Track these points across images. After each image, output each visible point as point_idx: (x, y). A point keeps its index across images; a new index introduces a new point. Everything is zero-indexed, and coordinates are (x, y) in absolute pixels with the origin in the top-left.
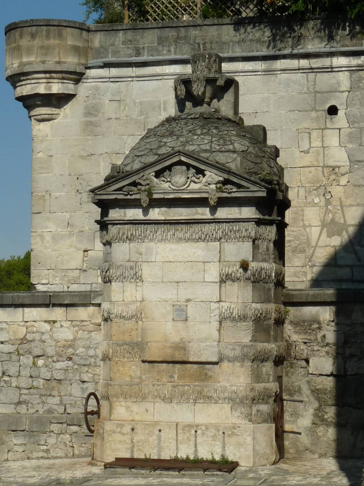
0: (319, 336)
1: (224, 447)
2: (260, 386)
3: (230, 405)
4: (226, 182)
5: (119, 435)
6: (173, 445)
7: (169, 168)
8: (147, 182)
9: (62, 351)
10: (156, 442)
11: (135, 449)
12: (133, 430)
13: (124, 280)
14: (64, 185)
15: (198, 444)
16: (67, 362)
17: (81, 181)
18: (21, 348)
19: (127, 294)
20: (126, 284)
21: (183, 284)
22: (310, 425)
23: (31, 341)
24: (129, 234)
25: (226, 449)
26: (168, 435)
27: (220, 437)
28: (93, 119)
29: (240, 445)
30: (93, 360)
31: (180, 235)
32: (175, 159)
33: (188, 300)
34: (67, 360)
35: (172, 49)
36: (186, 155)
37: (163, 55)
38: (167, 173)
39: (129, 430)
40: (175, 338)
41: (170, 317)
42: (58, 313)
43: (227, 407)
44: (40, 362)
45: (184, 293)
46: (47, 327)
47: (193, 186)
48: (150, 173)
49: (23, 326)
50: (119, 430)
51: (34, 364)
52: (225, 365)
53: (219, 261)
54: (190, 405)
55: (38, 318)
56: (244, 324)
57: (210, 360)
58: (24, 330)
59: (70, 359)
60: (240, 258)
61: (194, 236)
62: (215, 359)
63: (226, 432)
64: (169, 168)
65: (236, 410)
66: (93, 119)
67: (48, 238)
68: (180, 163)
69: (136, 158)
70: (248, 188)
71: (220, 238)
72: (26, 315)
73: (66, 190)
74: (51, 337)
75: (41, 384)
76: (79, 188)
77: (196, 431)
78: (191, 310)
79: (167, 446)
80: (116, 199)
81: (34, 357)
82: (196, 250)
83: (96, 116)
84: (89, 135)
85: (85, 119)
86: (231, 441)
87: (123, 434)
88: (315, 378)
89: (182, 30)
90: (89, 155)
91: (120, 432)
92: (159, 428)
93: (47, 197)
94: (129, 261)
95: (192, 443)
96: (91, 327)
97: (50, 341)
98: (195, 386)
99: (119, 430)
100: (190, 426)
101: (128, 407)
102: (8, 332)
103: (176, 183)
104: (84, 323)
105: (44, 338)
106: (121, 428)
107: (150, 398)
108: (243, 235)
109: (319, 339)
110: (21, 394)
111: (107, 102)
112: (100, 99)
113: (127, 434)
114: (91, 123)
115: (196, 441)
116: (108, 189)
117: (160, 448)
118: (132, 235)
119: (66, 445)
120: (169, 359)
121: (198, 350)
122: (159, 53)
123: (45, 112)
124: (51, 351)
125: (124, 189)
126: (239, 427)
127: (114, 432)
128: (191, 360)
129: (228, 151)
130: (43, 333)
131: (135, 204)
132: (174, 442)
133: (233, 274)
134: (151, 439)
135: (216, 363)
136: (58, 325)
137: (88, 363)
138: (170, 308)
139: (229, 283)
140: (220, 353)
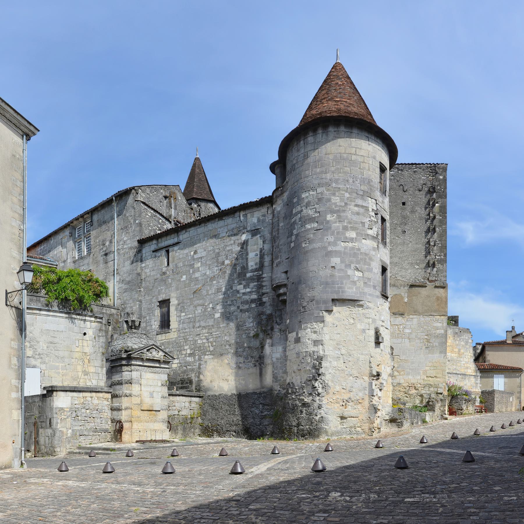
30: (104, 410)
42: (94, 394)
44: (88, 411)
46: (90, 399)
59: (97, 410)
124: (91, 408)
136: (93, 398)
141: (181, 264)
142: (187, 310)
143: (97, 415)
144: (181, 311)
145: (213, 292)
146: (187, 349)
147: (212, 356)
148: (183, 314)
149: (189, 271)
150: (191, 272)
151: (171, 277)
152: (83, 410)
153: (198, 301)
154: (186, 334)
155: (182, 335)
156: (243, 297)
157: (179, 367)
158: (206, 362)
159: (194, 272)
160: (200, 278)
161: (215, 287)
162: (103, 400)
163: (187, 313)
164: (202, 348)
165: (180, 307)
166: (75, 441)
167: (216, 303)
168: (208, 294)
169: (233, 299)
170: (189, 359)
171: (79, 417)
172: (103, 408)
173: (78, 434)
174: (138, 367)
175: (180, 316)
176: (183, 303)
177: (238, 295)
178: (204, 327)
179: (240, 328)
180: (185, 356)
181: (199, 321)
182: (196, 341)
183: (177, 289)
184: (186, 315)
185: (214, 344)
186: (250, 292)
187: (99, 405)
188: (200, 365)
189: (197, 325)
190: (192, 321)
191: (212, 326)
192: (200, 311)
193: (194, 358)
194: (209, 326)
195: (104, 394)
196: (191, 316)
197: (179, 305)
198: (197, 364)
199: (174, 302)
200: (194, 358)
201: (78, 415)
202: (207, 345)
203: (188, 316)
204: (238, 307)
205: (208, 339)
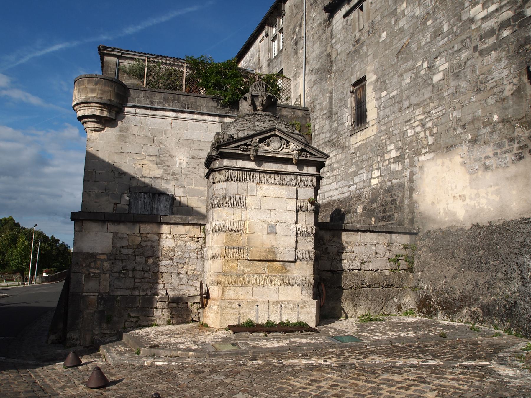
3: (300, 288)
4: (303, 150)
7: (269, 137)
9: (166, 254)
10: (255, 313)
11: (241, 319)
12: (240, 305)
15: (282, 314)
16: (169, 261)
18: (137, 251)
19: (236, 215)
20: (235, 209)
25: (300, 316)
28: (124, 134)
31: (271, 180)
32: (272, 133)
33: (277, 221)
34: (169, 259)
35: (171, 104)
36: (280, 130)
37: (166, 106)
39: (237, 306)
41: (266, 232)
43: (298, 289)
45: (274, 218)
47: (285, 151)
48: (257, 139)
49: (139, 236)
50: (230, 306)
51: (146, 261)
54: (275, 288)
55: (150, 231)
56: (309, 238)
57: (290, 260)
58: (140, 239)
59: (172, 259)
60: (307, 198)
64: (269, 137)
65: (304, 292)
66: (124, 134)
67: (93, 195)
68: (275, 135)
69: (238, 131)
72: (142, 229)
75: (150, 275)
78: (280, 229)
79: (263, 316)
81: (146, 258)
82: (282, 191)
83: (126, 132)
84: (121, 142)
85: (120, 133)
87: (233, 309)
89: (177, 95)
90: (120, 153)
91: (231, 308)
94: (237, 194)
96: (187, 239)
99: (230, 306)
100: (278, 302)
101: (235, 291)
102: (128, 240)
103: (275, 147)
104: (182, 236)
106: (232, 305)
109: (324, 250)
110: (135, 282)
111: (133, 126)
114: (123, 136)
115: (281, 311)
116: (230, 146)
117: (258, 318)
118: (240, 178)
121: (283, 253)
122: (163, 105)
123: (97, 126)
126: (308, 302)
127: (227, 307)
128: (278, 259)
130: (153, 242)
131: (247, 158)
137: (184, 262)
138: (265, 226)
141: (379, 18)
142: (389, 86)
144: (381, 90)
145: (429, 40)
146: (391, 151)
147: (431, 155)
148: (384, 93)
149: (390, 22)
150: (393, 23)
151: (367, 42)
153: (405, 64)
154: (389, 124)
155: (383, 128)
156: (483, 25)
157: (380, 183)
158: (422, 167)
159: (396, 22)
160: (406, 27)
161: (431, 30)
163: (390, 90)
164: (414, 144)
165: (379, 83)
167: (434, 56)
168: (420, 48)
169: (464, 37)
170: (395, 167)
175: (380, 98)
176: (383, 75)
177: (473, 27)
178: (417, 105)
179: (482, 87)
180: (390, 163)
181: (408, 97)
182: (405, 132)
183: (375, 57)
184: (387, 94)
185: (435, 130)
186: (497, 10)
188: (412, 174)
189: (406, 104)
190: (398, 101)
191: (430, 98)
192: (408, 80)
193: (403, 163)
194: (425, 100)
196: (395, 93)
197: (377, 80)
198: (408, 174)
199: (371, 78)
200: (403, 163)
202: (422, 135)
203: (392, 95)
204: (475, 48)
205: (423, 125)
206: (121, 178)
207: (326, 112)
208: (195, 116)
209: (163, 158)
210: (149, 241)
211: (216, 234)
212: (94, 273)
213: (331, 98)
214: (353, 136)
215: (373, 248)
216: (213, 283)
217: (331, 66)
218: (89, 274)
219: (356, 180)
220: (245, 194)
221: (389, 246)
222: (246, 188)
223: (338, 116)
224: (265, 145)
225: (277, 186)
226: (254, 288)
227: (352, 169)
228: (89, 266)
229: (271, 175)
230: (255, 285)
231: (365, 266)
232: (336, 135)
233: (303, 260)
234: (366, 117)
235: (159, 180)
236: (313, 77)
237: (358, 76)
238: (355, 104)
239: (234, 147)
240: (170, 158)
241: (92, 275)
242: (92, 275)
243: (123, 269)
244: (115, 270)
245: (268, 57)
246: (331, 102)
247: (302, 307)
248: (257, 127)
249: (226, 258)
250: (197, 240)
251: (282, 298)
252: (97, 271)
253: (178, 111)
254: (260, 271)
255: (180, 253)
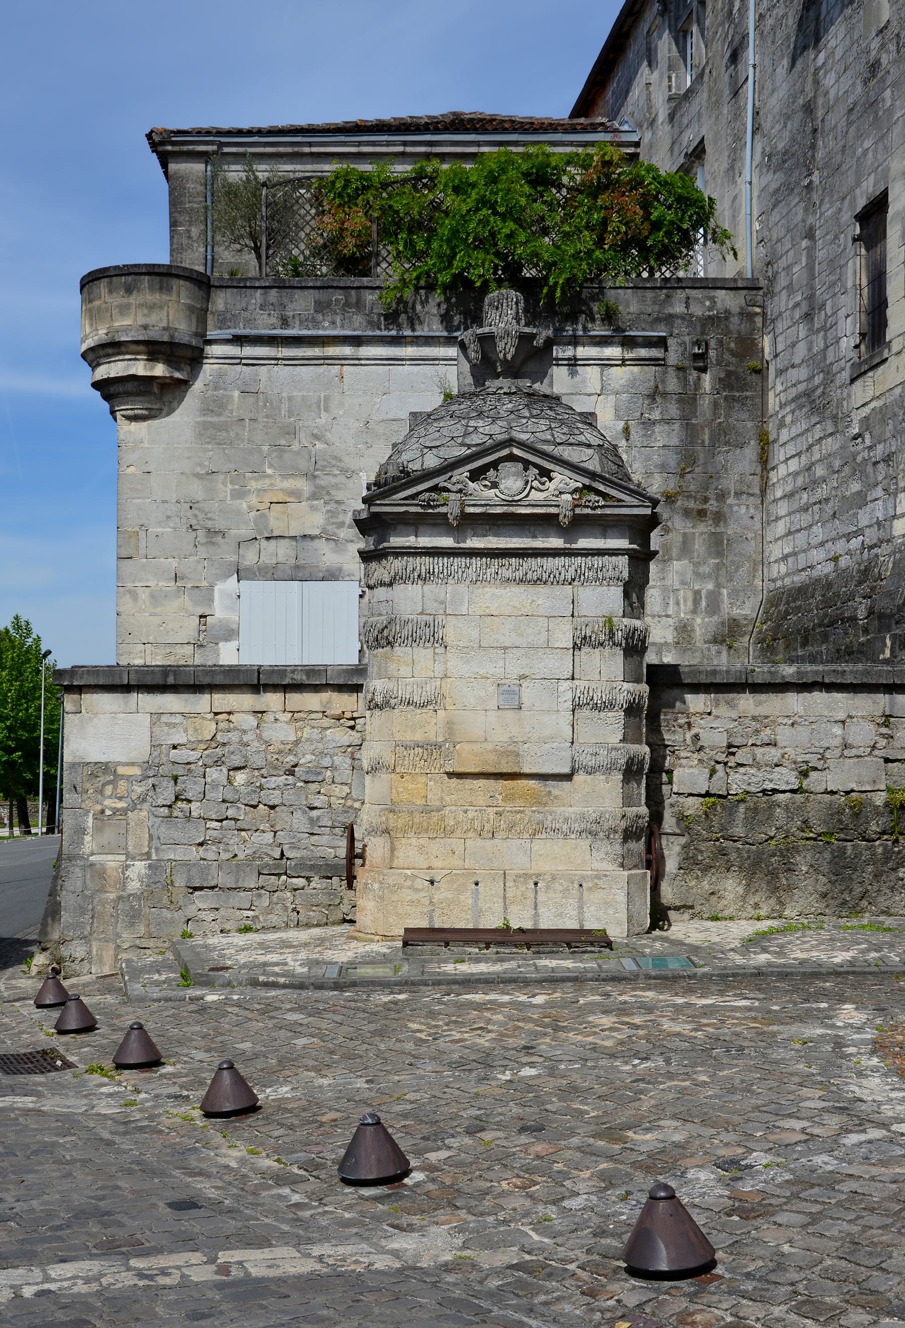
0: (688, 736)
1: (581, 908)
2: (632, 811)
3: (588, 842)
5: (409, 891)
6: (498, 907)
7: (495, 465)
8: (459, 486)
10: (470, 901)
13: (414, 645)
14: (169, 517)
17: (196, 512)
21: (514, 651)
22: (675, 871)
23: (224, 744)
24: (423, 570)
26: (490, 891)
27: (575, 892)
29: (607, 904)
30: (329, 773)
31: (506, 573)
33: (523, 677)
35: (338, 320)
37: (324, 328)
38: (491, 473)
40: (500, 736)
41: (493, 704)
42: (272, 700)
43: (585, 843)
44: (240, 778)
46: (252, 721)
47: (535, 496)
48: (462, 474)
50: (409, 883)
52: (579, 778)
53: (573, 616)
56: (610, 714)
57: (556, 771)
58: (214, 726)
59: (291, 772)
60: (604, 610)
61: (529, 577)
62: (566, 770)
63: (584, 885)
64: (495, 465)
67: (144, 595)
68: (512, 458)
69: (426, 450)
70: (619, 500)
71: (574, 580)
73: (172, 525)
74: (259, 737)
76: (194, 522)
77: (536, 884)
78: (528, 693)
79: (490, 908)
80: (406, 512)
83: (220, 415)
85: (202, 419)
86: (593, 898)
87: (417, 890)
88: (681, 799)
89: (353, 292)
90: (208, 474)
92: (475, 879)
93: (142, 534)
94: (421, 613)
95: (530, 902)
97: (256, 744)
98: (534, 812)
99: (409, 883)
100: (526, 876)
101: (421, 847)
103: (509, 489)
104: (313, 716)
105: (245, 739)
106: (413, 881)
107: (458, 833)
108: (608, 575)
109: (689, 741)
111: (236, 394)
112: (225, 389)
113: (422, 890)
116: (394, 497)
117: (479, 913)
119: (286, 908)
120: (492, 770)
122: (316, 324)
125: (422, 497)
126: (606, 876)
128: (526, 770)
129: (580, 444)
130: (245, 732)
131: (439, 523)
132: (501, 900)
133: (594, 636)
134: (462, 898)
135: (568, 777)
136: (269, 717)
137: (320, 778)
138: (492, 689)
139: (585, 649)
140: (573, 761)
143: (289, 796)
152: (216, 775)
162: (326, 722)
166: (167, 914)
171: (194, 806)
172: (326, 762)
173: (180, 881)
174: (427, 560)
187: (300, 749)
195: (325, 696)
201: (189, 795)
206: (213, 543)
207: (799, 298)
208: (410, 351)
209: (324, 481)
210: (235, 729)
211: (377, 712)
212: (115, 811)
213: (811, 251)
214: (858, 383)
215: (837, 730)
216: (372, 831)
217: (813, 147)
218: (103, 812)
219: (864, 518)
220: (441, 612)
221: (886, 725)
222: (442, 596)
223: (826, 314)
224: (485, 486)
225: (522, 588)
226: (469, 842)
227: (855, 487)
228: (101, 792)
229: (505, 561)
230: (470, 834)
231: (815, 781)
232: (821, 375)
233: (591, 771)
234: (886, 325)
235: (321, 544)
236: (774, 180)
237: (871, 190)
238: (868, 277)
239: (405, 499)
240: (342, 479)
241: (108, 812)
242: (108, 812)
243: (177, 798)
244: (160, 802)
245: (670, 87)
246: (810, 267)
247: (590, 889)
248: (473, 436)
249: (398, 770)
250: (352, 723)
251: (543, 866)
252: (121, 805)
253: (357, 341)
254: (482, 800)
255: (309, 757)
